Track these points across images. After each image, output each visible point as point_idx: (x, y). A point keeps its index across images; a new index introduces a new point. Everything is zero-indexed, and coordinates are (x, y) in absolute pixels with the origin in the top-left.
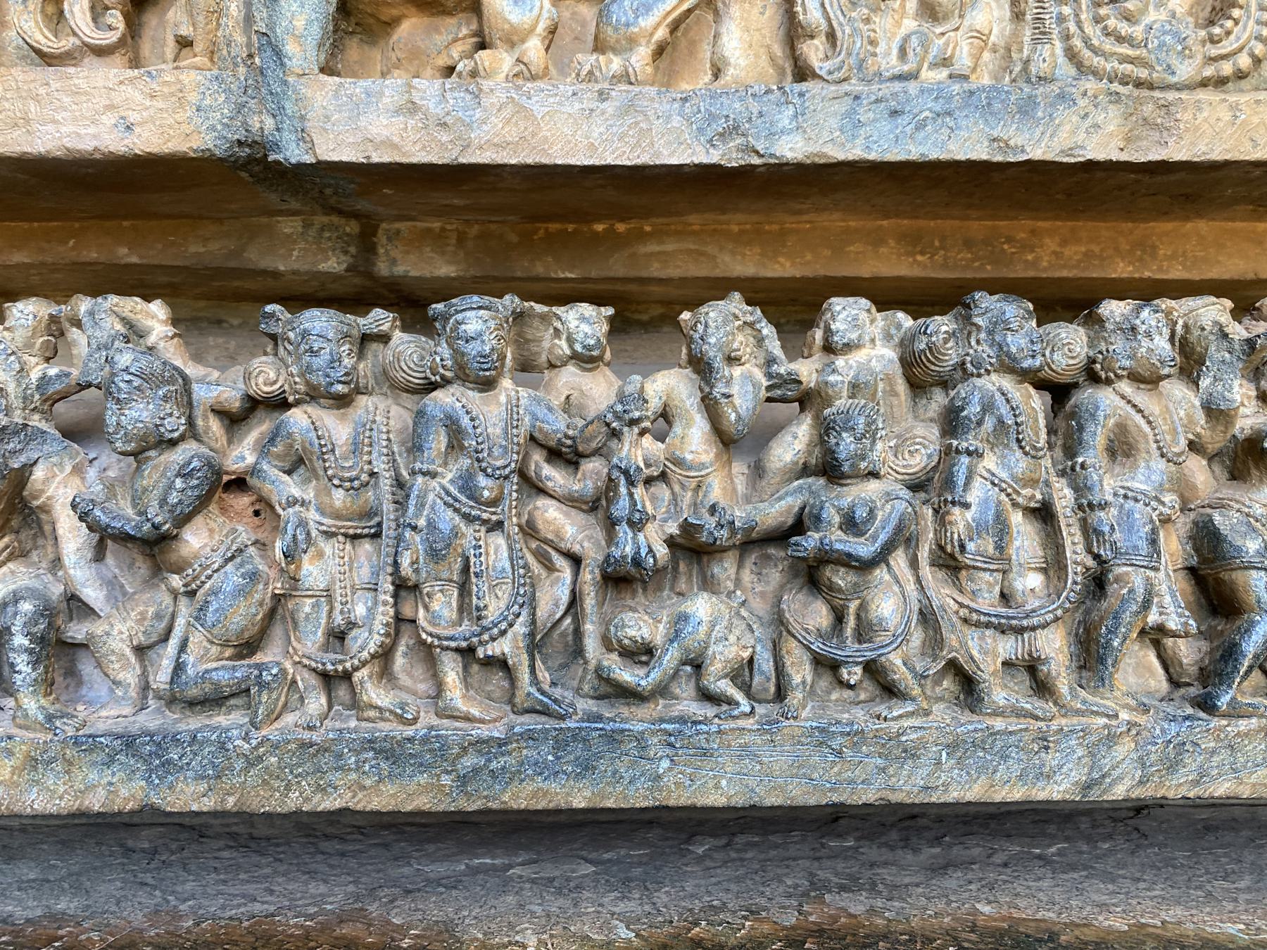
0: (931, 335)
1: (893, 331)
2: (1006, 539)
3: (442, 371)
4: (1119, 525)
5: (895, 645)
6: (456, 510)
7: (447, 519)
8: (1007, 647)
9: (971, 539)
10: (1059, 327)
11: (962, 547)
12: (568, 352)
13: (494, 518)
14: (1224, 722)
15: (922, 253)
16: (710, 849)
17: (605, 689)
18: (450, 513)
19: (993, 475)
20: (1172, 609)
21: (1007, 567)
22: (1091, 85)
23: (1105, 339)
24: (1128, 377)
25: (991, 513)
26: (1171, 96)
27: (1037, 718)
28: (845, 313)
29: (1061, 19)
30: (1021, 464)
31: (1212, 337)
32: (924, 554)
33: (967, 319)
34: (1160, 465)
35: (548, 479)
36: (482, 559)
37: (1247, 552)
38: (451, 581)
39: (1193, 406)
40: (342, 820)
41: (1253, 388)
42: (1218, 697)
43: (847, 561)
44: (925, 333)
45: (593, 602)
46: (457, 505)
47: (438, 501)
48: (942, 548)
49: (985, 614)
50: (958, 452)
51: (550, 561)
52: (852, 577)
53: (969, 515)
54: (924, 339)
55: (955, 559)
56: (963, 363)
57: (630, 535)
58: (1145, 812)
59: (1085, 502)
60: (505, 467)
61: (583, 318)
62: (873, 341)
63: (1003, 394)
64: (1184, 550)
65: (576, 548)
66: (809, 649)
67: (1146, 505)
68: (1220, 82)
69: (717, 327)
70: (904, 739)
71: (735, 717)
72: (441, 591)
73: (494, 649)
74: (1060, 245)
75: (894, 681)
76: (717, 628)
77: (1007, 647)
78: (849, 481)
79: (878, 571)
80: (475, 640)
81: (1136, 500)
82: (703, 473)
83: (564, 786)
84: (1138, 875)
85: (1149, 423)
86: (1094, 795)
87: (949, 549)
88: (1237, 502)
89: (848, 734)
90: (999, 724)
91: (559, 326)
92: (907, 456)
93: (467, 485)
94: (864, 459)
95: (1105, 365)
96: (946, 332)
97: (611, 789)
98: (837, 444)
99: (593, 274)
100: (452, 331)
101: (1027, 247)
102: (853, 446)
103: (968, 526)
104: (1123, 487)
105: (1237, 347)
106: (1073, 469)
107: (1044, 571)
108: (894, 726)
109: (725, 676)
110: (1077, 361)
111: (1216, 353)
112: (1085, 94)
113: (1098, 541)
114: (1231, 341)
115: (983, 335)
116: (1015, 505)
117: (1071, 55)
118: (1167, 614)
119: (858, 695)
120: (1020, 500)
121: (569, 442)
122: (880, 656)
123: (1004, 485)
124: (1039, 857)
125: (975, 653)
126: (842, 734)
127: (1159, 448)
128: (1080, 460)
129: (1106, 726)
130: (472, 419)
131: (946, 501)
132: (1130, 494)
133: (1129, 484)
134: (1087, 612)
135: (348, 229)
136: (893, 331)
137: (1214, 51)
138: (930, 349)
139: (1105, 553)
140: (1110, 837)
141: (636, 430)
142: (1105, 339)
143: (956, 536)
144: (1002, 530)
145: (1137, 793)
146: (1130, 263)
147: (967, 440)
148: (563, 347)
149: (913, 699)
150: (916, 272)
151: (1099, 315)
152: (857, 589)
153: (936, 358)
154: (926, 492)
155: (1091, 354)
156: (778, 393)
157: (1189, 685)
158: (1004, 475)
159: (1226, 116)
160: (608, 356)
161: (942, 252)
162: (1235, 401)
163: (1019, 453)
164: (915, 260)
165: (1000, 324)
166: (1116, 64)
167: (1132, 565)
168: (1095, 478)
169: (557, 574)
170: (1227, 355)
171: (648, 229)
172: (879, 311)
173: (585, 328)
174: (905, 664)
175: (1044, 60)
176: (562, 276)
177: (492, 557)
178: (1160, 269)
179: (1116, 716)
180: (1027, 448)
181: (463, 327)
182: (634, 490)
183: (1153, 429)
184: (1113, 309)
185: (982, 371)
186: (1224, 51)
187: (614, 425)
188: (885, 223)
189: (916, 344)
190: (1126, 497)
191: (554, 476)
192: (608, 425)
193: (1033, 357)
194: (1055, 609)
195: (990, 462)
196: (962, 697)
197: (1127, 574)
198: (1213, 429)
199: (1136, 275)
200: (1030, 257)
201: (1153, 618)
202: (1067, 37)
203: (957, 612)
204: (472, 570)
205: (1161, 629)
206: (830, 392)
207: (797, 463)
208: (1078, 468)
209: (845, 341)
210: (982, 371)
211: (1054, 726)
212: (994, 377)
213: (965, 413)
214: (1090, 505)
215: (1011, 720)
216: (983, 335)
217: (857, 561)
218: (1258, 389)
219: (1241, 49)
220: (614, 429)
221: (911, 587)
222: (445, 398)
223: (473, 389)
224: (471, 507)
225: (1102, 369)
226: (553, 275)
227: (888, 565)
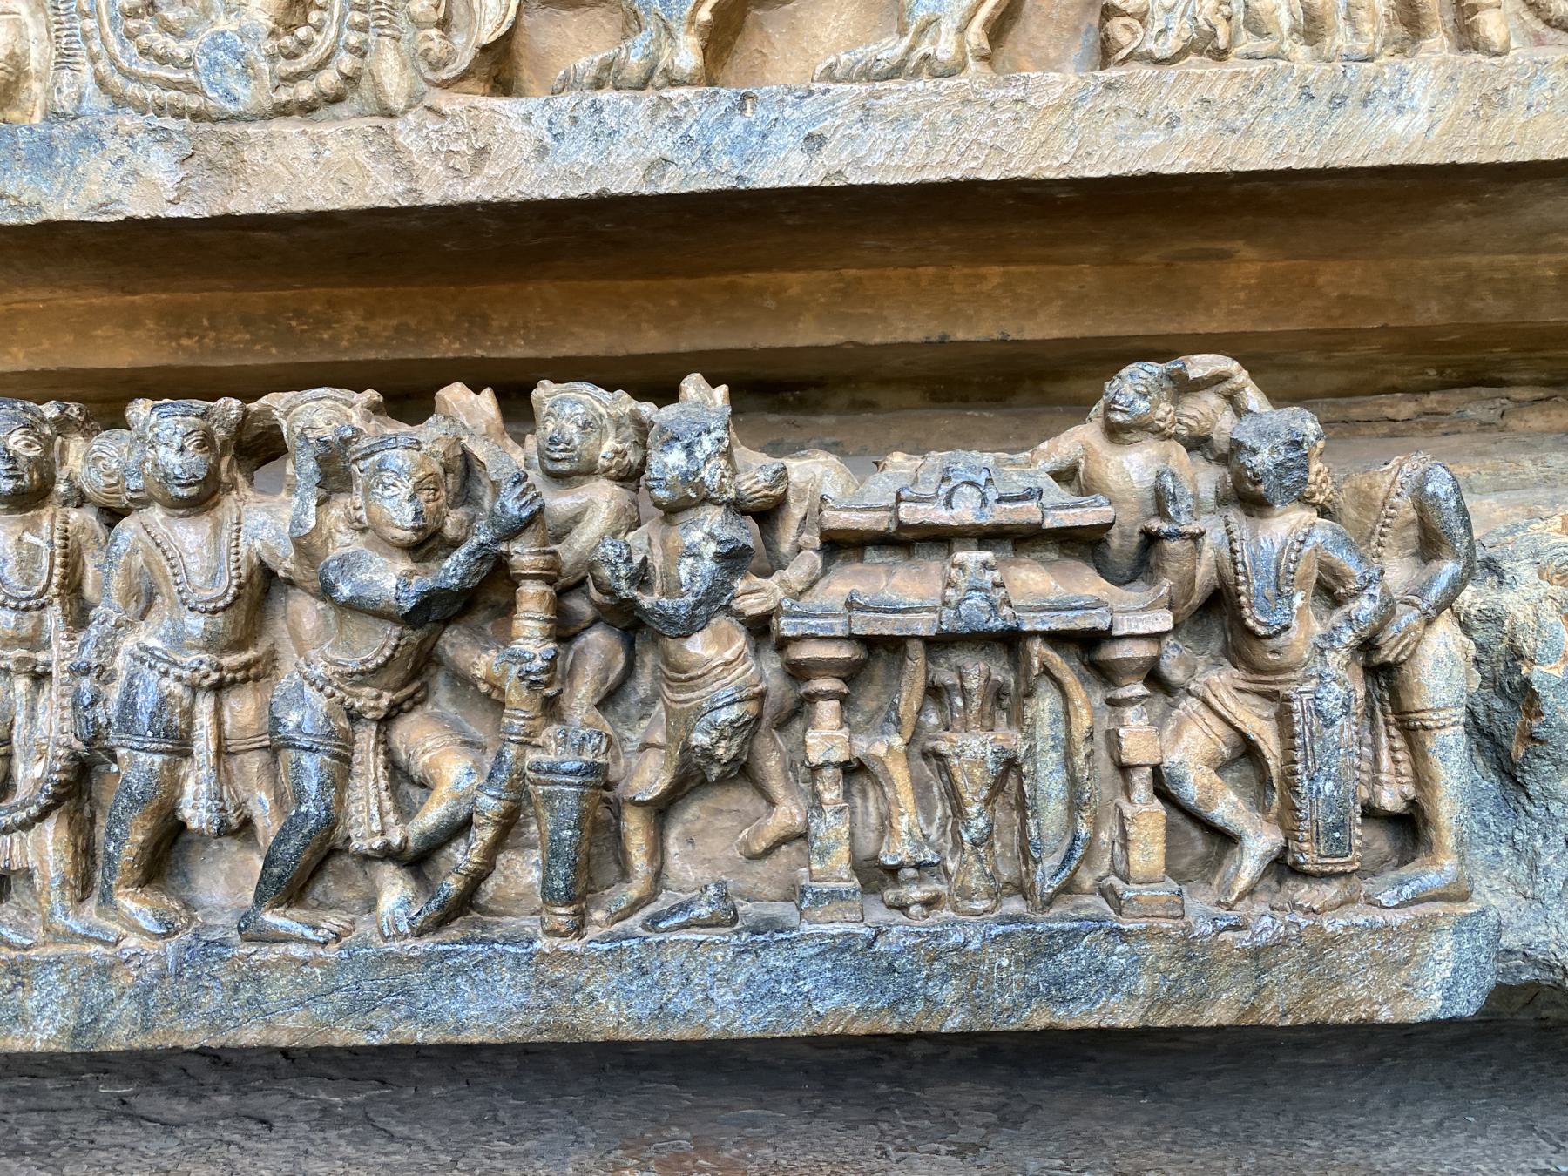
15: (189, 335)
20: (204, 801)
22: (129, 120)
26: (235, 129)
29: (86, 37)
31: (298, 443)
68: (307, 109)
74: (365, 319)
86: (87, 1044)
101: (323, 323)
112: (115, 133)
117: (101, 83)
137: (285, 67)
145: (137, 1044)
146: (457, 338)
150: (181, 360)
159: (306, 153)
161: (212, 334)
162: (305, 527)
164: (179, 345)
166: (157, 91)
175: (59, 91)
178: (495, 346)
183: (173, 567)
184: (139, 410)
186: (299, 68)
188: (137, 298)
198: (297, 561)
199: (465, 355)
200: (325, 336)
202: (94, 59)
219: (322, 65)
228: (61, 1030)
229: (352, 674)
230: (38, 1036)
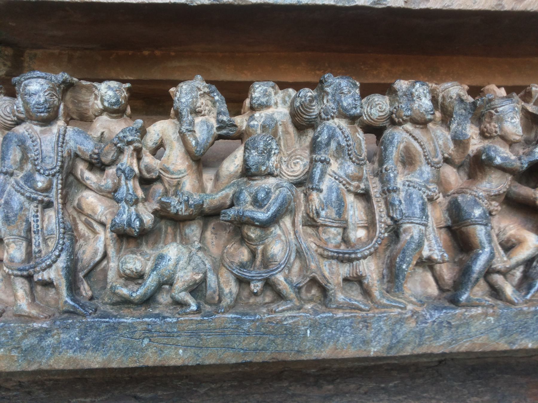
0: (301, 98)
1: (287, 99)
2: (342, 209)
3: (17, 114)
4: (405, 201)
5: (279, 270)
6: (22, 194)
7: (17, 199)
8: (345, 270)
9: (323, 209)
10: (375, 96)
11: (318, 214)
12: (101, 107)
13: (46, 199)
14: (464, 310)
15: (319, 70)
16: (208, 390)
17: (115, 299)
18: (19, 195)
19: (335, 174)
20: (436, 247)
21: (345, 225)
23: (398, 101)
24: (411, 122)
25: (334, 195)
27: (361, 310)
28: (260, 88)
30: (351, 168)
32: (299, 218)
33: (322, 90)
34: (427, 169)
35: (88, 179)
36: (39, 223)
37: (474, 216)
38: (20, 236)
39: (448, 139)
40: (13, 379)
41: (477, 129)
42: (461, 296)
43: (252, 222)
44: (299, 96)
45: (113, 250)
46: (22, 191)
47: (12, 189)
48: (308, 215)
49: (331, 251)
50: (316, 161)
51: (93, 227)
52: (258, 232)
53: (322, 196)
54: (298, 99)
55: (315, 221)
56: (320, 113)
57: (127, 208)
58: (444, 362)
59: (386, 188)
60: (52, 169)
61: (109, 88)
62: (276, 104)
63: (341, 129)
64: (445, 217)
65: (103, 219)
66: (232, 273)
67: (420, 190)
69: (186, 94)
70: (285, 323)
71: (187, 314)
72: (14, 242)
73: (45, 276)
75: (280, 290)
76: (181, 262)
77: (345, 270)
78: (256, 178)
79: (273, 229)
80: (31, 270)
81: (414, 187)
82: (180, 176)
83: (85, 355)
84: (433, 396)
85: (421, 146)
86: (392, 353)
87: (311, 215)
88: (470, 189)
89: (253, 321)
90: (340, 314)
91: (96, 92)
92: (293, 166)
93: (29, 179)
94: (263, 165)
95: (397, 114)
96: (310, 96)
97: (114, 357)
98: (249, 156)
99: (143, 77)
100: (23, 90)
102: (257, 158)
103: (321, 202)
104: (407, 181)
105: (468, 107)
106: (381, 172)
107: (367, 228)
108: (279, 316)
109: (185, 290)
110: (384, 113)
111: (458, 109)
113: (392, 210)
114: (466, 104)
115: (330, 97)
116: (349, 191)
118: (434, 251)
119: (264, 300)
120: (352, 188)
121: (95, 156)
122: (270, 275)
123: (341, 180)
124: (383, 388)
125: (327, 274)
126: (250, 321)
127: (426, 159)
128: (385, 166)
129: (400, 314)
130: (33, 142)
131: (309, 188)
132: (411, 184)
133: (411, 179)
134: (392, 251)
135: (6, 53)
136: (287, 99)
138: (301, 105)
139: (396, 216)
140: (423, 376)
141: (132, 148)
142: (398, 101)
143: (314, 207)
144: (341, 206)
147: (320, 154)
148: (99, 105)
149: (291, 300)
151: (394, 88)
152: (261, 239)
153: (305, 110)
154: (305, 186)
155: (391, 110)
156: (224, 132)
157: (448, 290)
158: (342, 174)
160: (129, 110)
163: (349, 163)
165: (339, 90)
167: (412, 223)
168: (392, 175)
169: (98, 235)
170: (464, 111)
171: (173, 54)
172: (281, 89)
173: (111, 93)
174: (286, 280)
176: (126, 78)
177: (46, 222)
179: (405, 308)
180: (354, 159)
181: (28, 88)
182: (128, 182)
183: (423, 149)
185: (329, 117)
187: (119, 145)
189: (295, 103)
190: (409, 186)
191: (91, 177)
192: (116, 145)
193: (356, 108)
194: (370, 248)
195: (334, 166)
196: (322, 299)
197: (409, 228)
198: (457, 151)
201: (426, 253)
203: (316, 251)
204: (32, 229)
205: (430, 259)
206: (251, 130)
207: (237, 172)
208: (384, 171)
209: (259, 102)
210: (329, 117)
211: (371, 314)
212: (336, 120)
213: (319, 139)
214: (389, 190)
215: (347, 311)
216: (330, 97)
217: (258, 222)
218: (480, 129)
220: (119, 148)
221: (292, 236)
222: (21, 129)
223: (36, 125)
224: (31, 193)
225: (396, 117)
226: (121, 78)
227: (279, 225)
228: (383, 347)
229: (491, 196)
230: (372, 349)
